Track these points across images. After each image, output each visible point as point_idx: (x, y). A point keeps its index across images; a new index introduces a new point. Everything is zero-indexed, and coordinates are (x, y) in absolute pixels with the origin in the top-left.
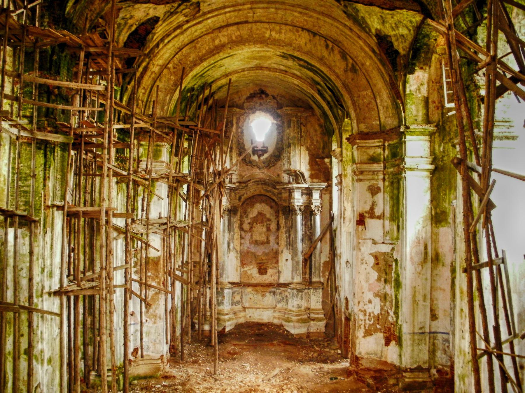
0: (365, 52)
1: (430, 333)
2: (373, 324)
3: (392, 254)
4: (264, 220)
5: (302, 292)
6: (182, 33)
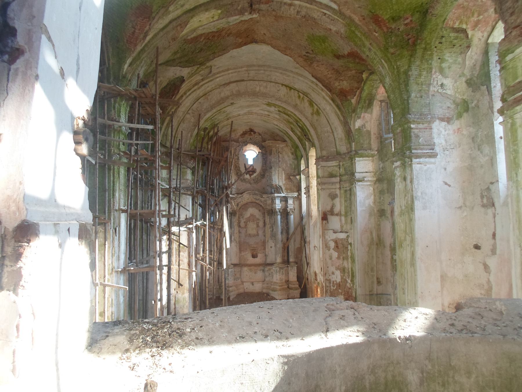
0: (327, 100)
1: (377, 294)
2: (336, 289)
3: (348, 240)
5: (283, 269)
6: (199, 88)
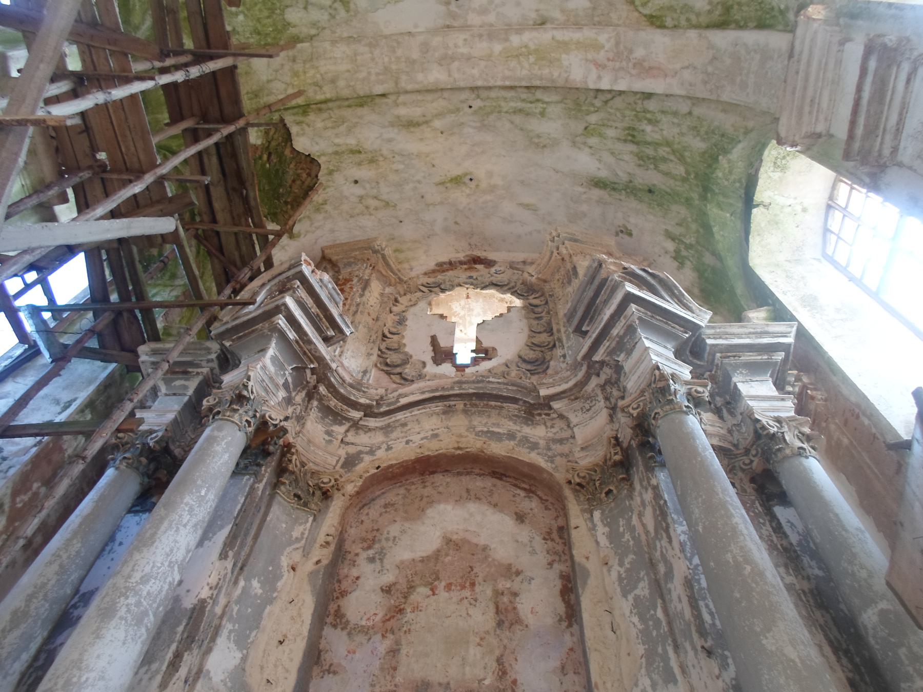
4: (480, 571)
